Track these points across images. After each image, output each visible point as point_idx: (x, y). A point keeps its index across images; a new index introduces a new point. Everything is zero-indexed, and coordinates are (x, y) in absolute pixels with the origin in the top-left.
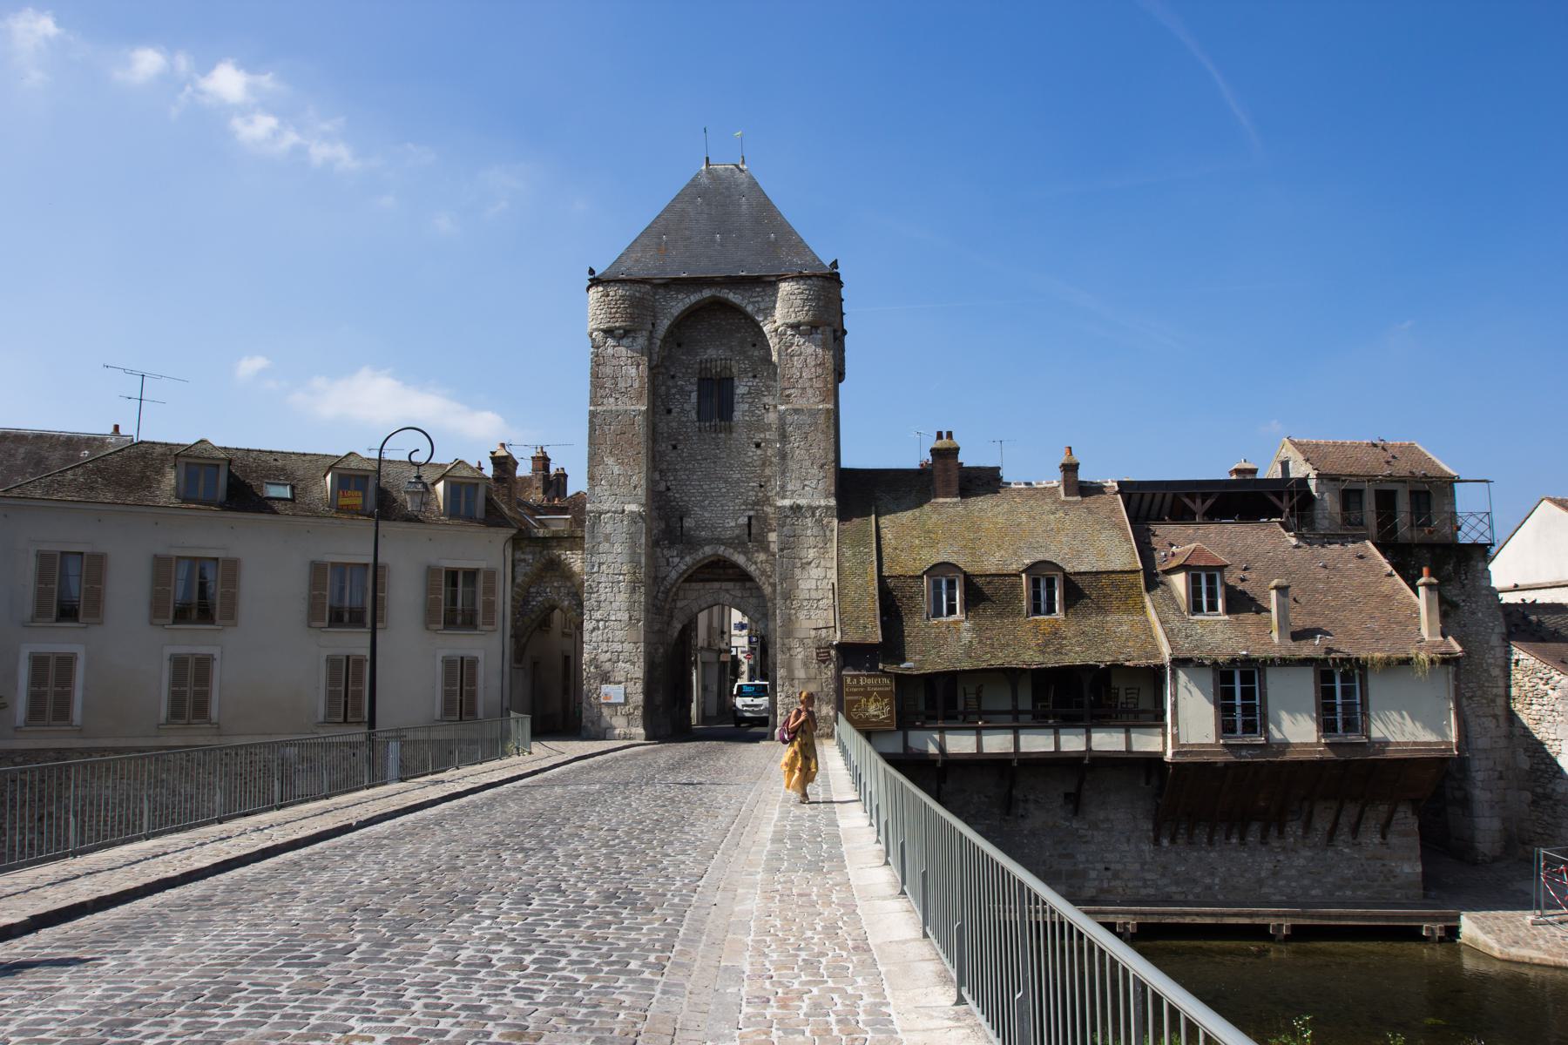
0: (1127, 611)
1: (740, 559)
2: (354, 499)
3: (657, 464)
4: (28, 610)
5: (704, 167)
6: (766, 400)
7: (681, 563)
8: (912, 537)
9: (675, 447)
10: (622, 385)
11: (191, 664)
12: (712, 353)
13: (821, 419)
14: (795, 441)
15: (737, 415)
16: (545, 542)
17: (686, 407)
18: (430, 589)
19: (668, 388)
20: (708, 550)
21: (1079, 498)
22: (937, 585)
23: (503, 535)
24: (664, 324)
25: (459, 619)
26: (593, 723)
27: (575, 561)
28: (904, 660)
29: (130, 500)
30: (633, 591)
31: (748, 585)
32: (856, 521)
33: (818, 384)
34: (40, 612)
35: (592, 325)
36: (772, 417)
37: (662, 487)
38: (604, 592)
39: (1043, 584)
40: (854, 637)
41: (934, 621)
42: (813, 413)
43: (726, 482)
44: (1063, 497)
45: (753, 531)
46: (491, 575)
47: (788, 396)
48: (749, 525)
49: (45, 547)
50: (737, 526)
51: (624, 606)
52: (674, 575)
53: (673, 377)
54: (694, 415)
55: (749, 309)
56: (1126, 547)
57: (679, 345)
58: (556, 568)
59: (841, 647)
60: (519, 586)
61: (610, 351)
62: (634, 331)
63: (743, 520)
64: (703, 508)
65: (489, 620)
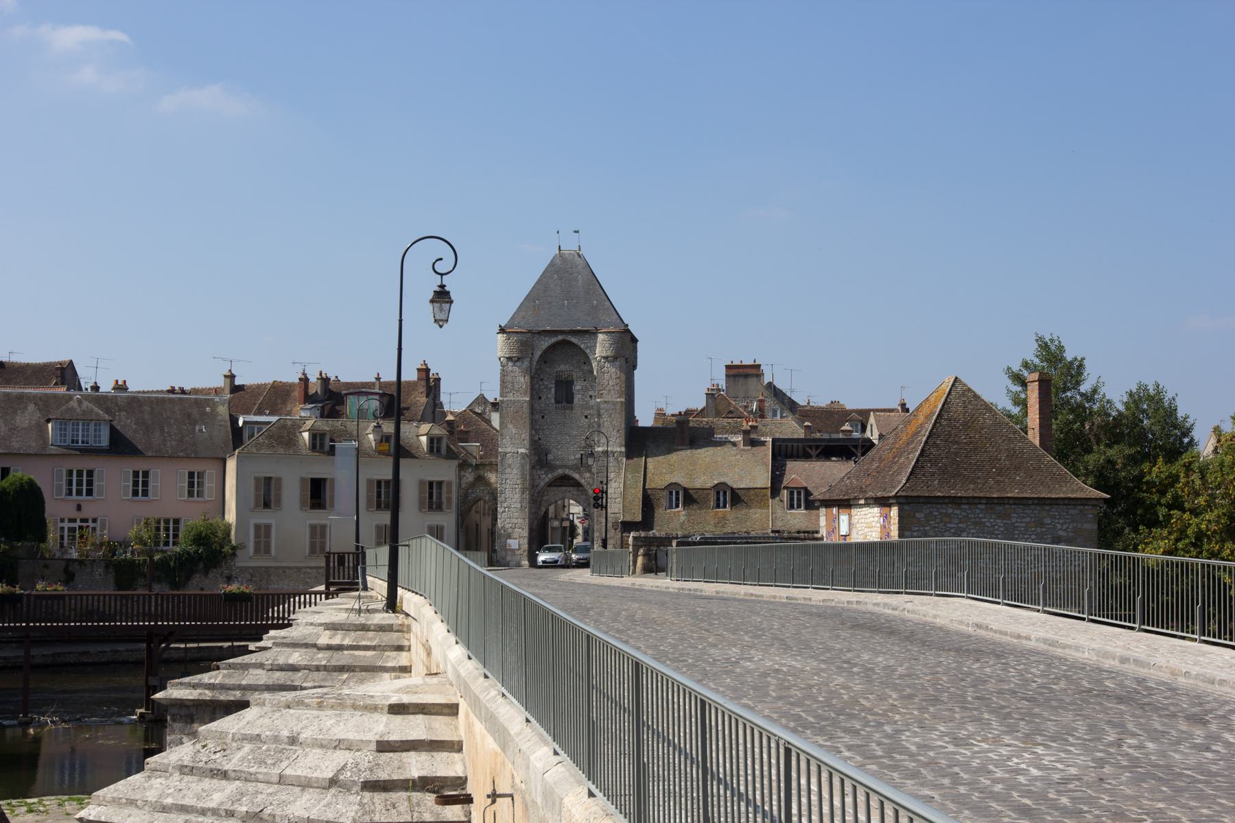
0: (760, 508)
1: (577, 476)
2: (385, 447)
3: (534, 426)
4: (252, 503)
5: (557, 252)
6: (590, 393)
7: (547, 478)
8: (663, 468)
9: (543, 417)
10: (516, 386)
11: (318, 529)
12: (562, 367)
13: (618, 407)
14: (605, 417)
15: (576, 400)
16: (477, 467)
17: (549, 396)
18: (421, 491)
19: (540, 385)
20: (560, 471)
21: (750, 447)
22: (671, 493)
23: (454, 464)
24: (538, 353)
25: (434, 507)
26: (503, 559)
27: (492, 477)
28: (652, 529)
29: (291, 452)
30: (523, 493)
31: (581, 488)
32: (635, 459)
33: (617, 388)
34: (257, 505)
35: (500, 354)
36: (592, 402)
37: (536, 438)
38: (508, 493)
39: (721, 494)
40: (628, 519)
41: (668, 511)
42: (614, 403)
43: (569, 436)
44: (742, 447)
45: (584, 461)
46: (449, 484)
47: (602, 394)
48: (581, 458)
49: (257, 475)
50: (575, 459)
51: (518, 500)
52: (542, 484)
53: (542, 380)
54: (553, 401)
55: (582, 346)
56: (766, 475)
57: (545, 362)
58: (480, 479)
59: (623, 523)
60: (463, 489)
61: (510, 368)
62: (523, 358)
63: (579, 456)
64: (558, 449)
65: (449, 507)
